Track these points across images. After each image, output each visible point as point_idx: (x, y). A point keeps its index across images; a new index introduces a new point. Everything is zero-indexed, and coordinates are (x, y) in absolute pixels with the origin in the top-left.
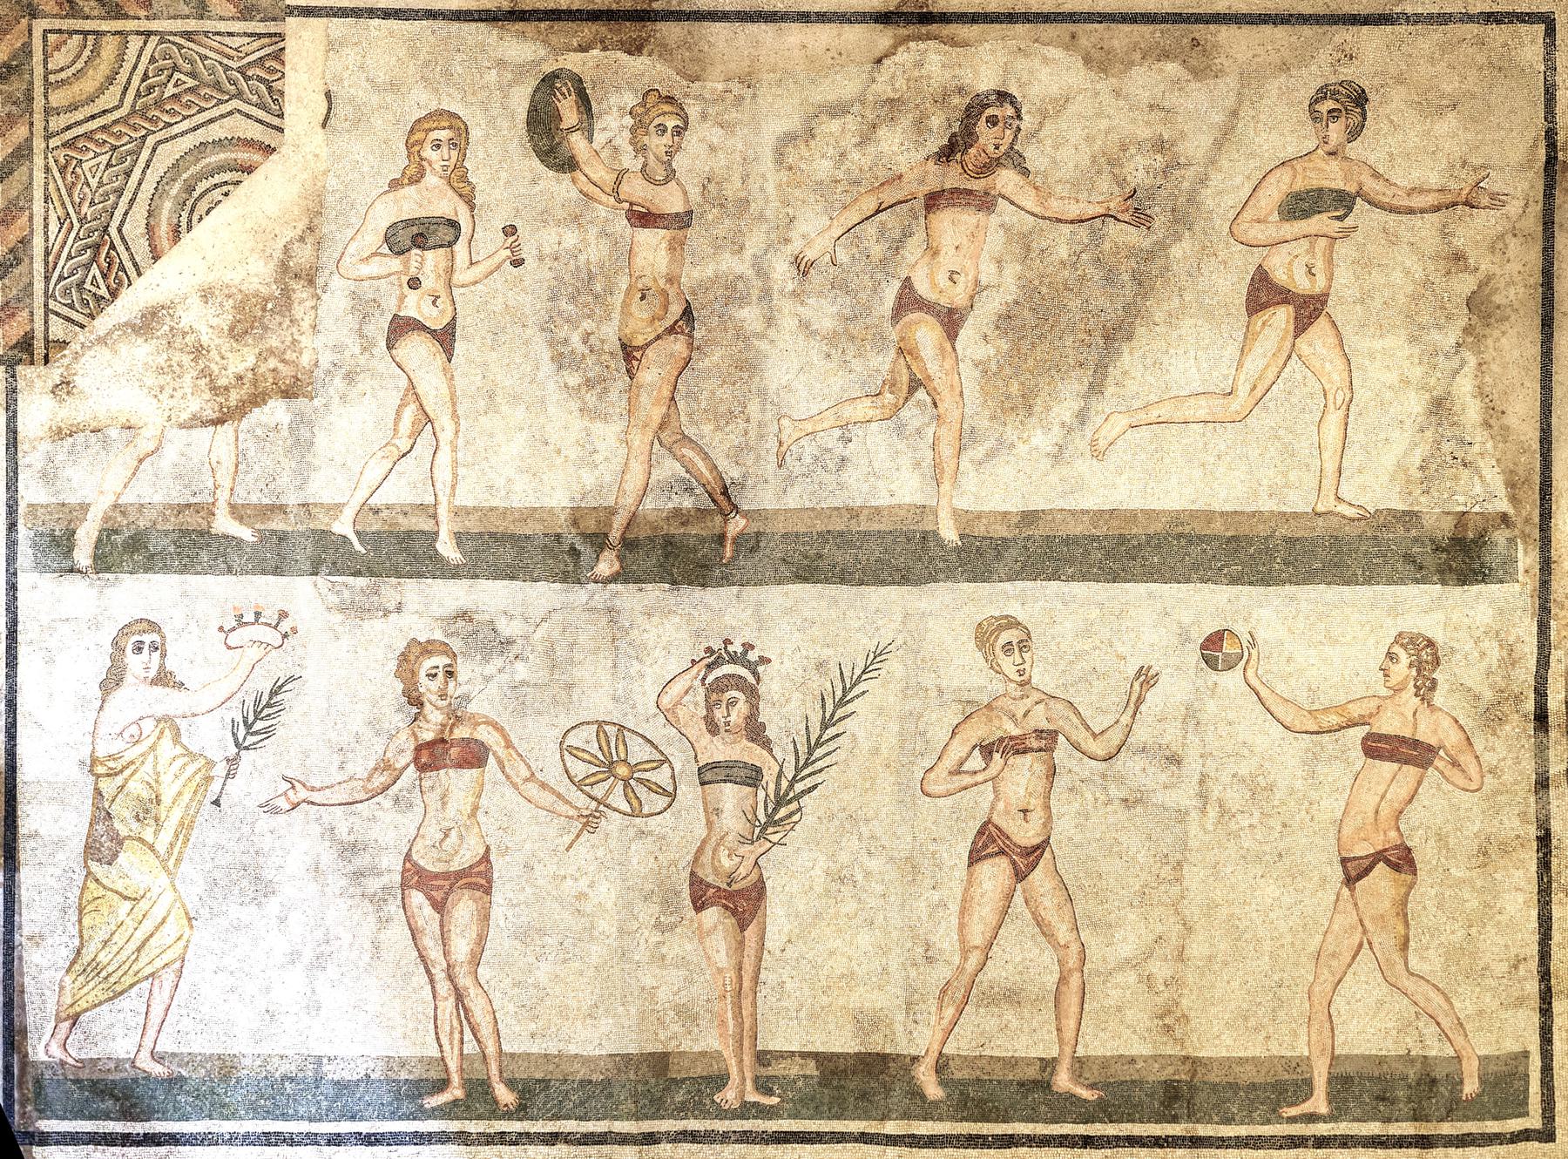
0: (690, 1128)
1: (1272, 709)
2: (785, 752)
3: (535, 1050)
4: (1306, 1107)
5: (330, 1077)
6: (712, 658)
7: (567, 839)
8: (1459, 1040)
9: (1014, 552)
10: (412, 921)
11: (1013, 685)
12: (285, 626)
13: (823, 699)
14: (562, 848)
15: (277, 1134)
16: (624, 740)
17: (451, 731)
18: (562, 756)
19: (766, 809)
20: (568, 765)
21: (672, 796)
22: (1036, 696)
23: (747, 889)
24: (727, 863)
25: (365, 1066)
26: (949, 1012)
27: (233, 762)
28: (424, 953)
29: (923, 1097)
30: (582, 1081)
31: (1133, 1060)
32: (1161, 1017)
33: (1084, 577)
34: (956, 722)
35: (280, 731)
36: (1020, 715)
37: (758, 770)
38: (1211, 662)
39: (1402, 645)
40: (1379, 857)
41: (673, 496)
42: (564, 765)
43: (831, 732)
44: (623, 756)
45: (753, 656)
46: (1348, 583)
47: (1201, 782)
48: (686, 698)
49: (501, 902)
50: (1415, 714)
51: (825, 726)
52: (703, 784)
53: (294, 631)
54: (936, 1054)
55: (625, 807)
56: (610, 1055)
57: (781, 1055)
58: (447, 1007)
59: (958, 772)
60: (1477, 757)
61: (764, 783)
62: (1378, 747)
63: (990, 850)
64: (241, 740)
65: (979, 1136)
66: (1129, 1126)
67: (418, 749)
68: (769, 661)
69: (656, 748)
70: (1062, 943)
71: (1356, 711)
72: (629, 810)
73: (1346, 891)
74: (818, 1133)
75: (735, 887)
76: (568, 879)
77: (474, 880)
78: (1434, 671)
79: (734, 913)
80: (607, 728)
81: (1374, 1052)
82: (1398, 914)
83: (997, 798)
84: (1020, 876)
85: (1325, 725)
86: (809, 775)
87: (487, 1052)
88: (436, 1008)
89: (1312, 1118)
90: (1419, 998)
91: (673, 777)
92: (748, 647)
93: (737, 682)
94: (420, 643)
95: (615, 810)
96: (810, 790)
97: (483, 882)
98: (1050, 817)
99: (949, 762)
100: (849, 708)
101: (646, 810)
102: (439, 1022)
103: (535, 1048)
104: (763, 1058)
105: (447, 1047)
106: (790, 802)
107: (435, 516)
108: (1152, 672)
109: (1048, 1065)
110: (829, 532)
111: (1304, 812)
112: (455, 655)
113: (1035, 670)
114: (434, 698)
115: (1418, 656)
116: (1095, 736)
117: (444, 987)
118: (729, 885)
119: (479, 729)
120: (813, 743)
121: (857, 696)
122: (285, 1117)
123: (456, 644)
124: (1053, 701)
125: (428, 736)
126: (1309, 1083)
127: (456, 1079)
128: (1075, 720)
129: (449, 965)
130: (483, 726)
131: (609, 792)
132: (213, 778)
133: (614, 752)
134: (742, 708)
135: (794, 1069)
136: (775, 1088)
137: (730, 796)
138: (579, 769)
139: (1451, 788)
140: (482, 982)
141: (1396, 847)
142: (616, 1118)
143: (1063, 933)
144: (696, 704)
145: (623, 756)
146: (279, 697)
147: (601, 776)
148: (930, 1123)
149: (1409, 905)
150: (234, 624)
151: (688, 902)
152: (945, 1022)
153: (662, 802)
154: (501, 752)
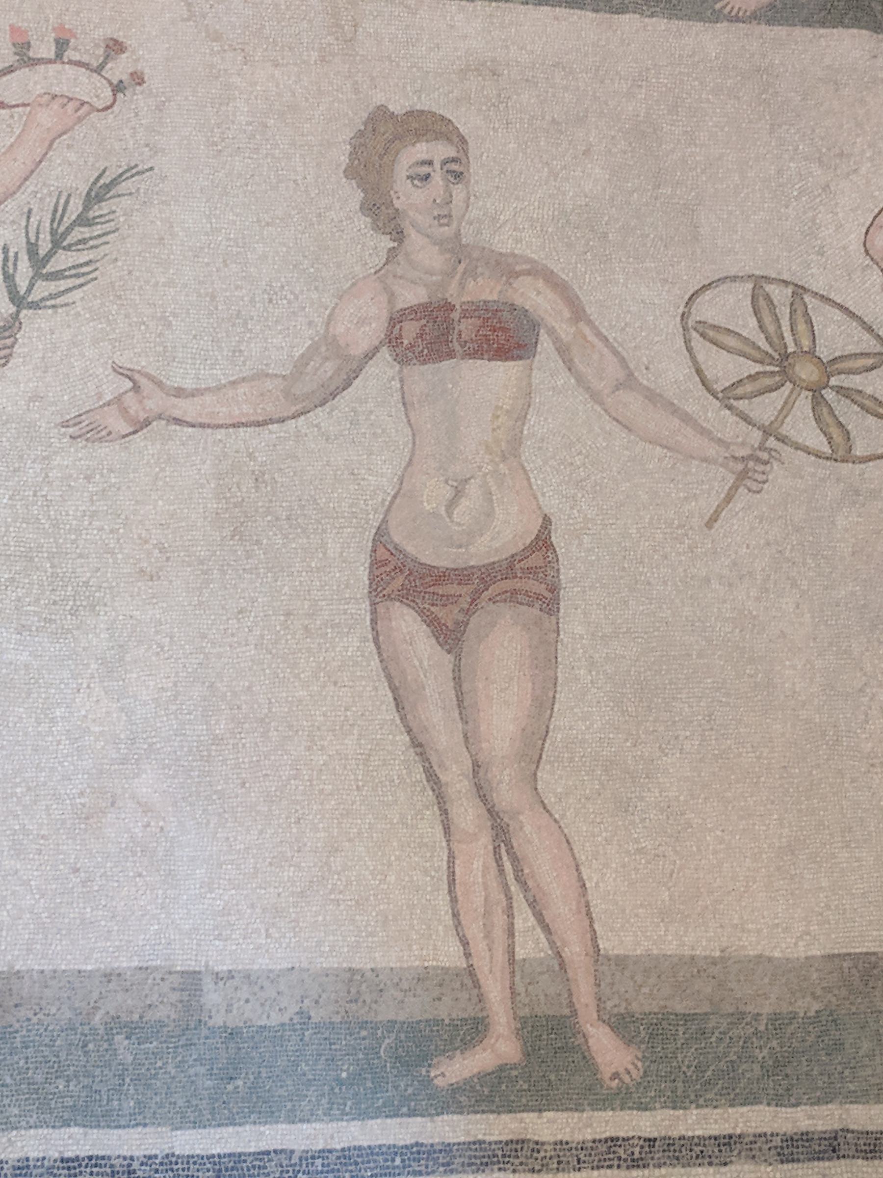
3: (671, 948)
5: (218, 1020)
12: (119, 69)
16: (806, 313)
17: (462, 285)
18: (687, 342)
20: (701, 358)
28: (421, 738)
30: (775, 1017)
42: (693, 358)
44: (806, 343)
49: (579, 630)
53: (138, 79)
55: (816, 440)
56: (830, 957)
67: (395, 320)
69: (869, 329)
72: (827, 450)
76: (715, 585)
77: (518, 584)
80: (770, 288)
87: (566, 953)
88: (451, 858)
95: (797, 447)
97: (542, 589)
101: (858, 452)
102: (459, 890)
105: (479, 946)
114: (419, 218)
129: (476, 766)
130: (529, 279)
131: (787, 406)
133: (787, 335)
140: (550, 800)
142: (854, 1098)
146: (104, 208)
147: (768, 381)
150: (12, 59)
154: (565, 331)
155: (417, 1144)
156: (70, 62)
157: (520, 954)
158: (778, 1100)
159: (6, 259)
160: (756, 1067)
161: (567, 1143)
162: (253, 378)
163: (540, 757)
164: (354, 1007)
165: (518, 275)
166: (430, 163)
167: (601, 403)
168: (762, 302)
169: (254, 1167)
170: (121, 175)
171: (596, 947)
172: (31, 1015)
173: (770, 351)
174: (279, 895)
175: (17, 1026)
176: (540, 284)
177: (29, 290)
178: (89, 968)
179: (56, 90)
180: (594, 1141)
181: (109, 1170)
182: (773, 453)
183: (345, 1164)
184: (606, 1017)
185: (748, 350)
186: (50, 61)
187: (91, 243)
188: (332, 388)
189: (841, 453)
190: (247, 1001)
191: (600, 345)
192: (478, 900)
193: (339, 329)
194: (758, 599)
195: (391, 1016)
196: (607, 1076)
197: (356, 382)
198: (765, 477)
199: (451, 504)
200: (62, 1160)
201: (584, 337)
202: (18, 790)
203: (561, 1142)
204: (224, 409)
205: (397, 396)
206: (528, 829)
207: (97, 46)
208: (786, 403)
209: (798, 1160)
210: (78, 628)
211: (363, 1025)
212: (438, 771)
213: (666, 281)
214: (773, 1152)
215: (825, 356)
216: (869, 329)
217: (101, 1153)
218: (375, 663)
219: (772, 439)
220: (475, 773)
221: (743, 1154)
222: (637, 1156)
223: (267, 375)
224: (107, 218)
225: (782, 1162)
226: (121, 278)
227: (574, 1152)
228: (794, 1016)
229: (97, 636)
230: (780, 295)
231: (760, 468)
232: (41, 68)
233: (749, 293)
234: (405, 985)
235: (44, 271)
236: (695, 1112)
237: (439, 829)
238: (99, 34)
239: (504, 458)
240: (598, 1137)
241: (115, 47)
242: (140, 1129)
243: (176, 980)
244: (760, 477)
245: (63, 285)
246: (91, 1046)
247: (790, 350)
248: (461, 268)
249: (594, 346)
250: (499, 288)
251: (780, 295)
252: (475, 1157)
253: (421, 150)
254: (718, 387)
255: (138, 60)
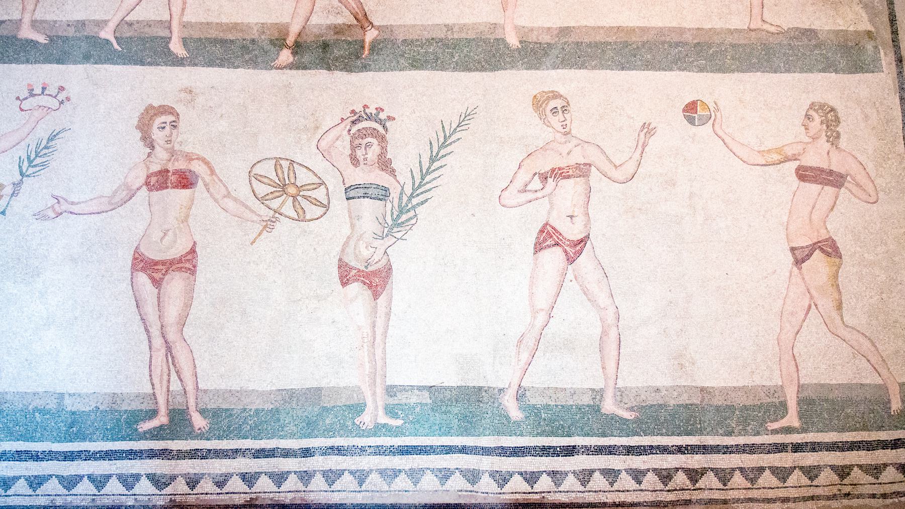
0: (336, 445)
1: (734, 150)
2: (404, 177)
3: (223, 387)
4: (783, 423)
5: (69, 409)
6: (355, 118)
7: (252, 237)
8: (884, 372)
9: (555, 52)
10: (137, 293)
11: (560, 135)
12: (61, 96)
13: (431, 143)
14: (248, 243)
15: (27, 452)
19: (392, 214)
20: (254, 186)
21: (327, 207)
22: (575, 142)
23: (379, 271)
24: (366, 253)
25: (96, 401)
26: (525, 356)
27: (17, 185)
29: (508, 418)
30: (257, 410)
31: (658, 390)
32: (675, 358)
33: (602, 67)
34: (522, 158)
35: (53, 164)
36: (564, 154)
37: (386, 189)
38: (691, 121)
39: (815, 110)
40: (814, 247)
41: (331, 17)
42: (252, 187)
43: (437, 164)
44: (293, 181)
45: (382, 116)
46: (776, 72)
47: (690, 197)
48: (338, 143)
49: (203, 280)
50: (828, 153)
51: (433, 160)
52: (348, 199)
53: (68, 99)
54: (516, 387)
57: (404, 389)
58: (160, 357)
59: (524, 191)
60: (873, 181)
61: (391, 198)
62: (805, 174)
63: (548, 243)
64: (24, 171)
65: (550, 448)
66: (659, 438)
68: (394, 119)
69: (316, 175)
70: (602, 306)
71: (790, 152)
72: (296, 217)
73: (795, 269)
74: (431, 447)
75: (370, 269)
78: (837, 126)
79: (370, 286)
80: (283, 162)
81: (828, 381)
82: (833, 285)
83: (552, 207)
84: (571, 260)
85: (770, 160)
86: (422, 193)
88: (151, 356)
89: (788, 430)
90: (854, 344)
91: (328, 194)
92: (380, 110)
93: (374, 133)
94: (154, 107)
95: (286, 216)
96: (422, 203)
97: (191, 267)
98: (589, 220)
99: (519, 184)
100: (449, 149)
101: (308, 217)
102: (153, 367)
103: (223, 386)
104: (391, 391)
105: (157, 386)
106: (408, 211)
107: (170, 28)
108: (650, 128)
109: (598, 393)
110: (433, 39)
111: (762, 217)
112: (178, 115)
113: (573, 125)
115: (826, 117)
116: (616, 167)
117: (158, 342)
118: (366, 267)
119: (192, 162)
120: (424, 171)
121: (454, 142)
122: (32, 439)
123: (179, 108)
124: (586, 145)
125: (155, 168)
126: (784, 405)
127: (163, 410)
128: (603, 157)
129: (162, 326)
130: (196, 161)
131: (283, 203)
132: (2, 196)
134: (375, 149)
135: (414, 399)
136: (400, 412)
137: (368, 208)
138: (262, 189)
139: (857, 201)
141: (826, 240)
142: (281, 437)
143: (603, 299)
144: (344, 148)
145: (293, 181)
147: (277, 194)
148: (514, 438)
149: (840, 279)
150: (27, 95)
151: (337, 280)
152: (522, 363)
153: (320, 211)
154: (208, 179)
155: (131, 450)
156: (47, 95)
157: (171, 389)
158: (255, 438)
159: (20, 162)
160: (249, 427)
161: (181, 450)
162: (98, 198)
163: (185, 323)
164: (114, 405)
165: (193, 159)
166: (166, 123)
167: (218, 203)
168: (278, 167)
169: (77, 456)
170: (59, 132)
171: (197, 387)
172: (9, 406)
173: (280, 183)
174: (92, 369)
175: (5, 409)
176: (200, 163)
177: (26, 171)
178: (29, 391)
179: (40, 104)
180: (190, 450)
181: (31, 455)
182: (277, 219)
183: (107, 456)
184: (198, 410)
185: (272, 183)
186: (40, 95)
187: (48, 155)
188: (125, 200)
189: (302, 218)
190: (79, 403)
191: (219, 183)
192: (158, 372)
193: (129, 180)
194: (267, 269)
195: (126, 408)
196: (197, 429)
197: (133, 198)
198: (273, 227)
199: (162, 239)
200: (17, 451)
201: (214, 180)
202: (11, 334)
203: (179, 450)
204: (87, 208)
205: (147, 203)
206: (178, 348)
207: (56, 89)
208: (283, 201)
209: (260, 458)
210: (33, 282)
211: (116, 411)
212: (149, 328)
213: (245, 160)
214: (252, 455)
215: (299, 184)
216: (316, 175)
217: (29, 450)
218: (131, 292)
219: (277, 214)
220: (162, 329)
221: (241, 455)
222: (204, 455)
223: (103, 197)
224: (54, 146)
225: (254, 458)
226: (57, 166)
227: (183, 453)
228: (263, 410)
229: (39, 284)
230: (285, 164)
231: (272, 224)
232: (36, 97)
233: (274, 164)
234: (132, 398)
235: (32, 165)
236: (226, 441)
237: (148, 347)
238: (57, 85)
239: (183, 222)
240: (192, 449)
241: (62, 89)
242: (41, 442)
243: (56, 396)
244: (271, 227)
245: (38, 169)
246: (28, 416)
247: (286, 183)
248: (173, 158)
249: (217, 183)
250: (186, 164)
251: (285, 164)
252: (150, 454)
253: (163, 118)
254: (260, 196)
255: (69, 93)
